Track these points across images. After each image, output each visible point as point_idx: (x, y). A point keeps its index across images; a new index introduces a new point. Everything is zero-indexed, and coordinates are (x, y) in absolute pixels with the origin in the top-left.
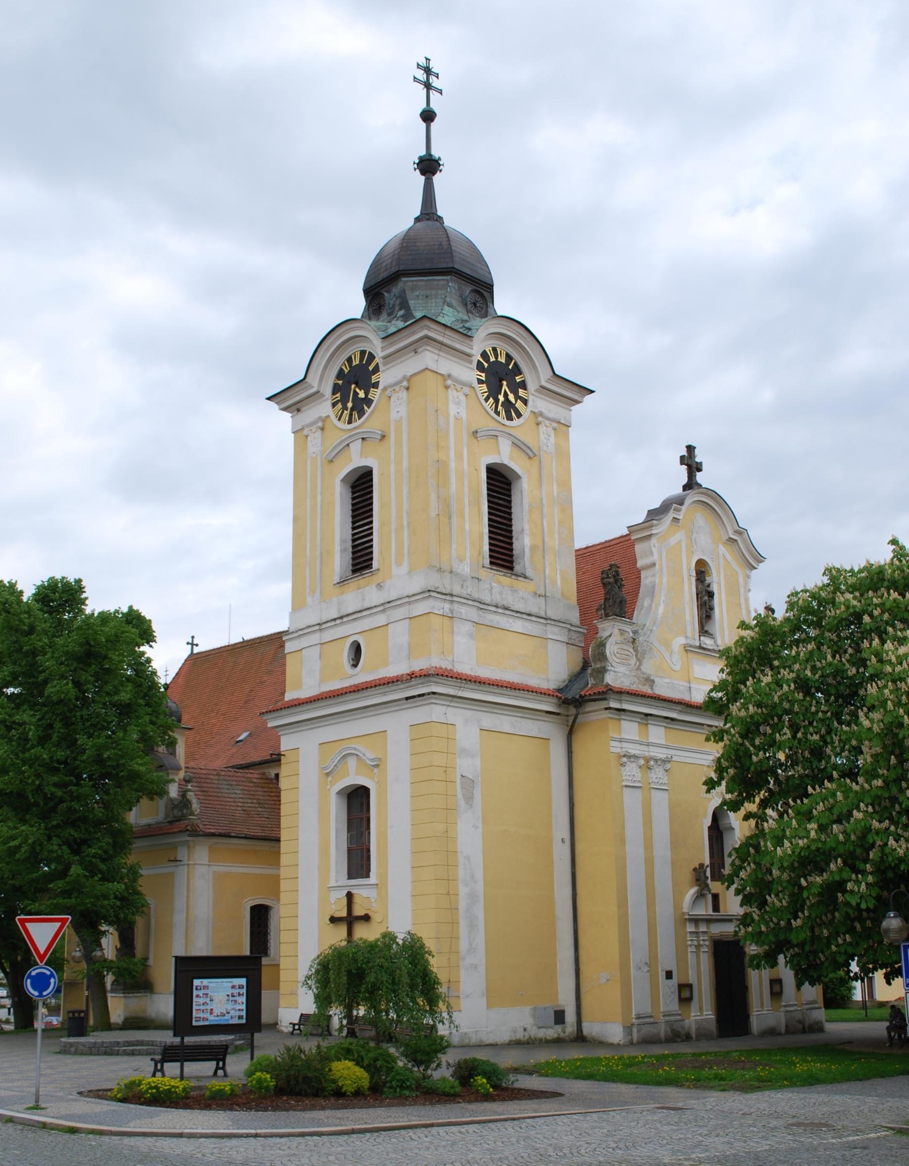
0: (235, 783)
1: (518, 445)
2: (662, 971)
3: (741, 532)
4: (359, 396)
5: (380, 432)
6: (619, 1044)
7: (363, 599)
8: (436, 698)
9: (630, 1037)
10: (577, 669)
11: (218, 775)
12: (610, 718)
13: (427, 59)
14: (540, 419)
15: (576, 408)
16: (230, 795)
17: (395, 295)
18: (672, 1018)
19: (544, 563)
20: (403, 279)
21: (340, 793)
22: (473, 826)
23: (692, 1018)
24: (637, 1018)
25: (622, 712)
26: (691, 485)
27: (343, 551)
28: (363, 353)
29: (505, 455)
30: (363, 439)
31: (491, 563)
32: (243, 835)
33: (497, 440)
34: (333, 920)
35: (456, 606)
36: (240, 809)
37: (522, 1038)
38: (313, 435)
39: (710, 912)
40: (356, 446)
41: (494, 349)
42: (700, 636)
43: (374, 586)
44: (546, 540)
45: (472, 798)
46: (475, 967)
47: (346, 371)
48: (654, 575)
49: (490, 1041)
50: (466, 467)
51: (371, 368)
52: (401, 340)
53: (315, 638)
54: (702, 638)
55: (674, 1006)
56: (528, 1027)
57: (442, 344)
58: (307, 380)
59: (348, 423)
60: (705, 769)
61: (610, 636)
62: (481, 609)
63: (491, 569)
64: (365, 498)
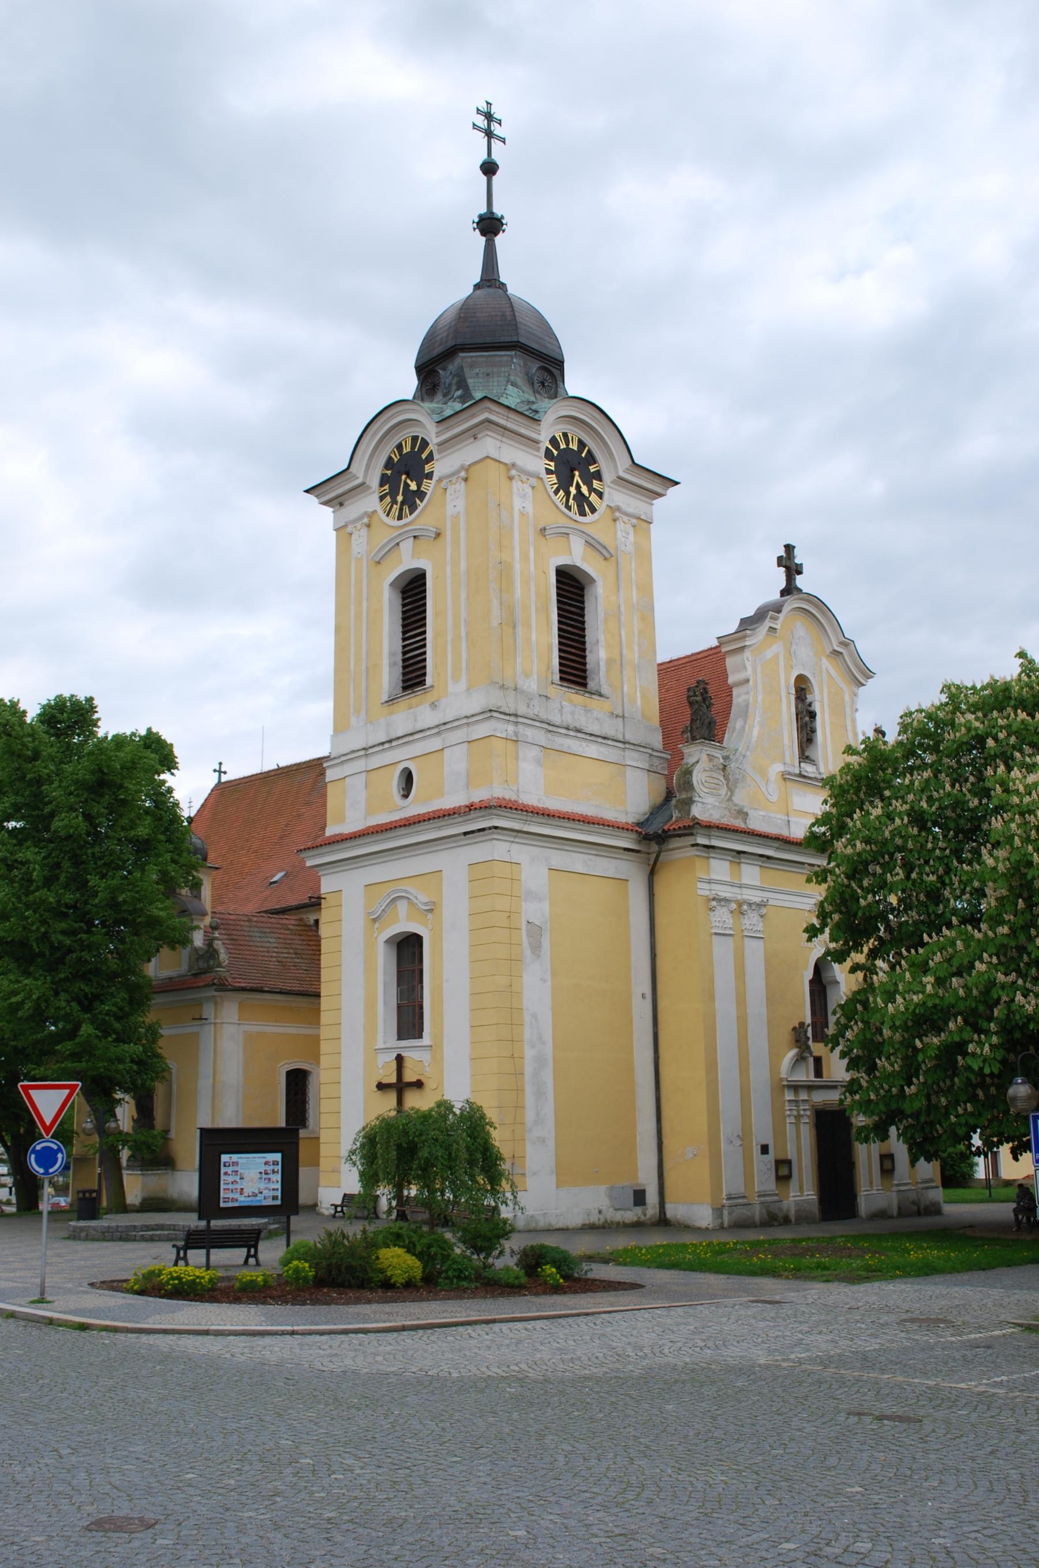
0: (268, 930)
1: (592, 544)
2: (757, 1145)
3: (847, 643)
4: (411, 488)
5: (435, 530)
6: (707, 1229)
7: (415, 720)
8: (498, 833)
9: (720, 1220)
10: (660, 800)
11: (249, 921)
12: (698, 856)
13: (488, 103)
14: (617, 514)
15: (658, 502)
16: (262, 944)
17: (451, 373)
18: (768, 1199)
19: (622, 679)
20: (461, 355)
21: (387, 942)
22: (541, 979)
23: (791, 1199)
24: (728, 1199)
25: (711, 850)
26: (789, 590)
27: (392, 665)
28: (415, 439)
29: (577, 556)
30: (415, 537)
31: (561, 679)
32: (278, 990)
33: (568, 538)
34: (381, 1086)
35: (521, 728)
36: (274, 959)
37: (597, 1222)
38: (358, 532)
39: (812, 1077)
40: (407, 545)
41: (565, 435)
42: (800, 762)
43: (427, 705)
44: (624, 652)
45: (540, 947)
46: (543, 1140)
47: (396, 460)
48: (748, 693)
49: (560, 1225)
50: (532, 569)
51: (424, 456)
52: (458, 424)
53: (360, 765)
54: (802, 765)
55: (771, 1185)
56: (604, 1208)
57: (505, 428)
58: (351, 470)
59: (398, 519)
60: (806, 914)
61: (697, 762)
62: (550, 731)
63: (562, 686)
64: (417, 604)
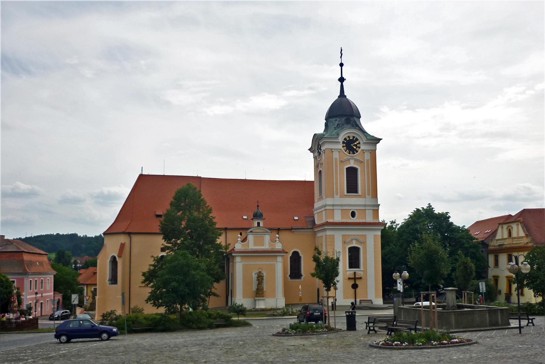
28: (354, 137)
34: (349, 278)
47: (348, 139)
53: (340, 208)
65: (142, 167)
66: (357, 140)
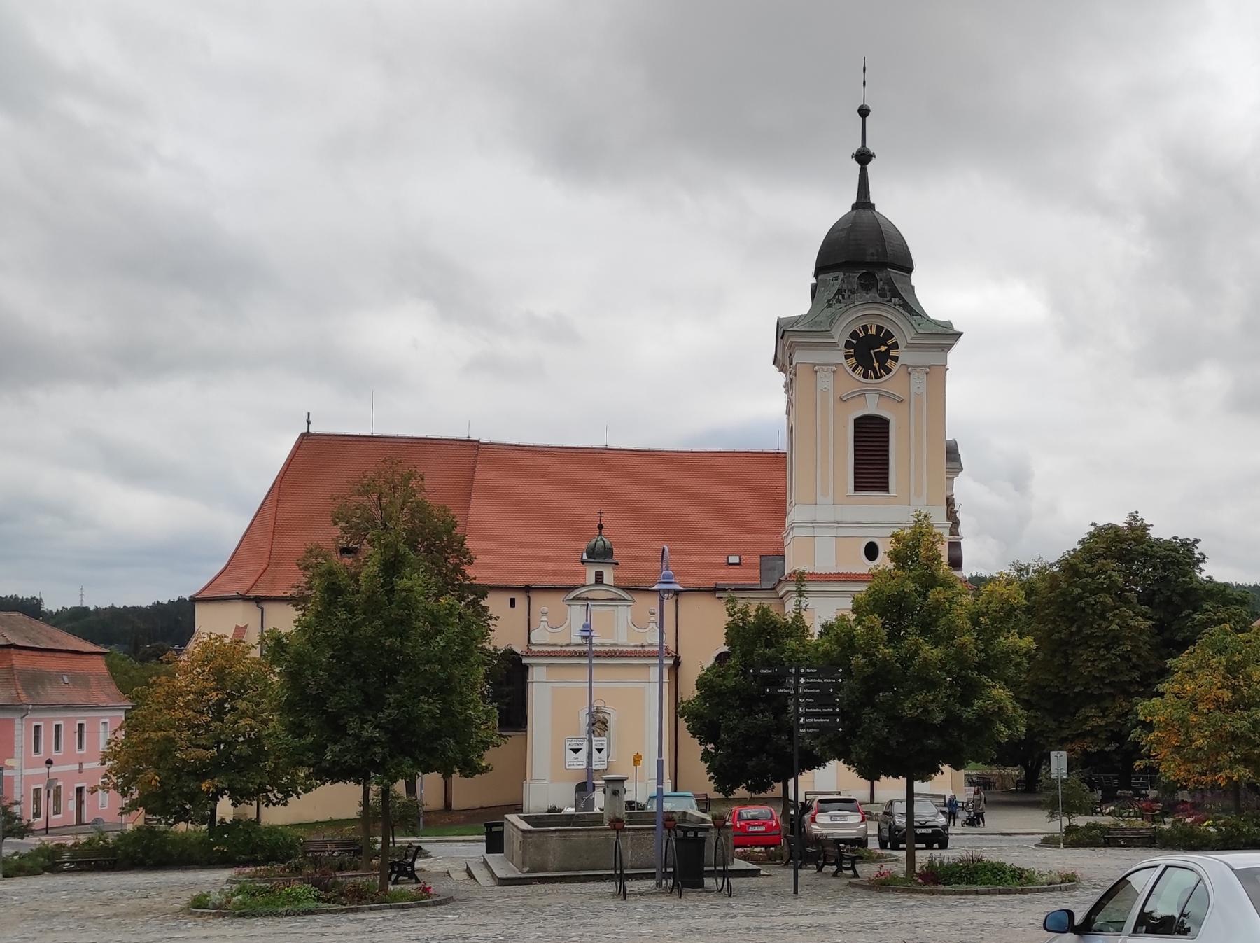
20: (889, 269)
47: (861, 336)
53: (833, 532)
65: (309, 414)
66: (889, 335)
